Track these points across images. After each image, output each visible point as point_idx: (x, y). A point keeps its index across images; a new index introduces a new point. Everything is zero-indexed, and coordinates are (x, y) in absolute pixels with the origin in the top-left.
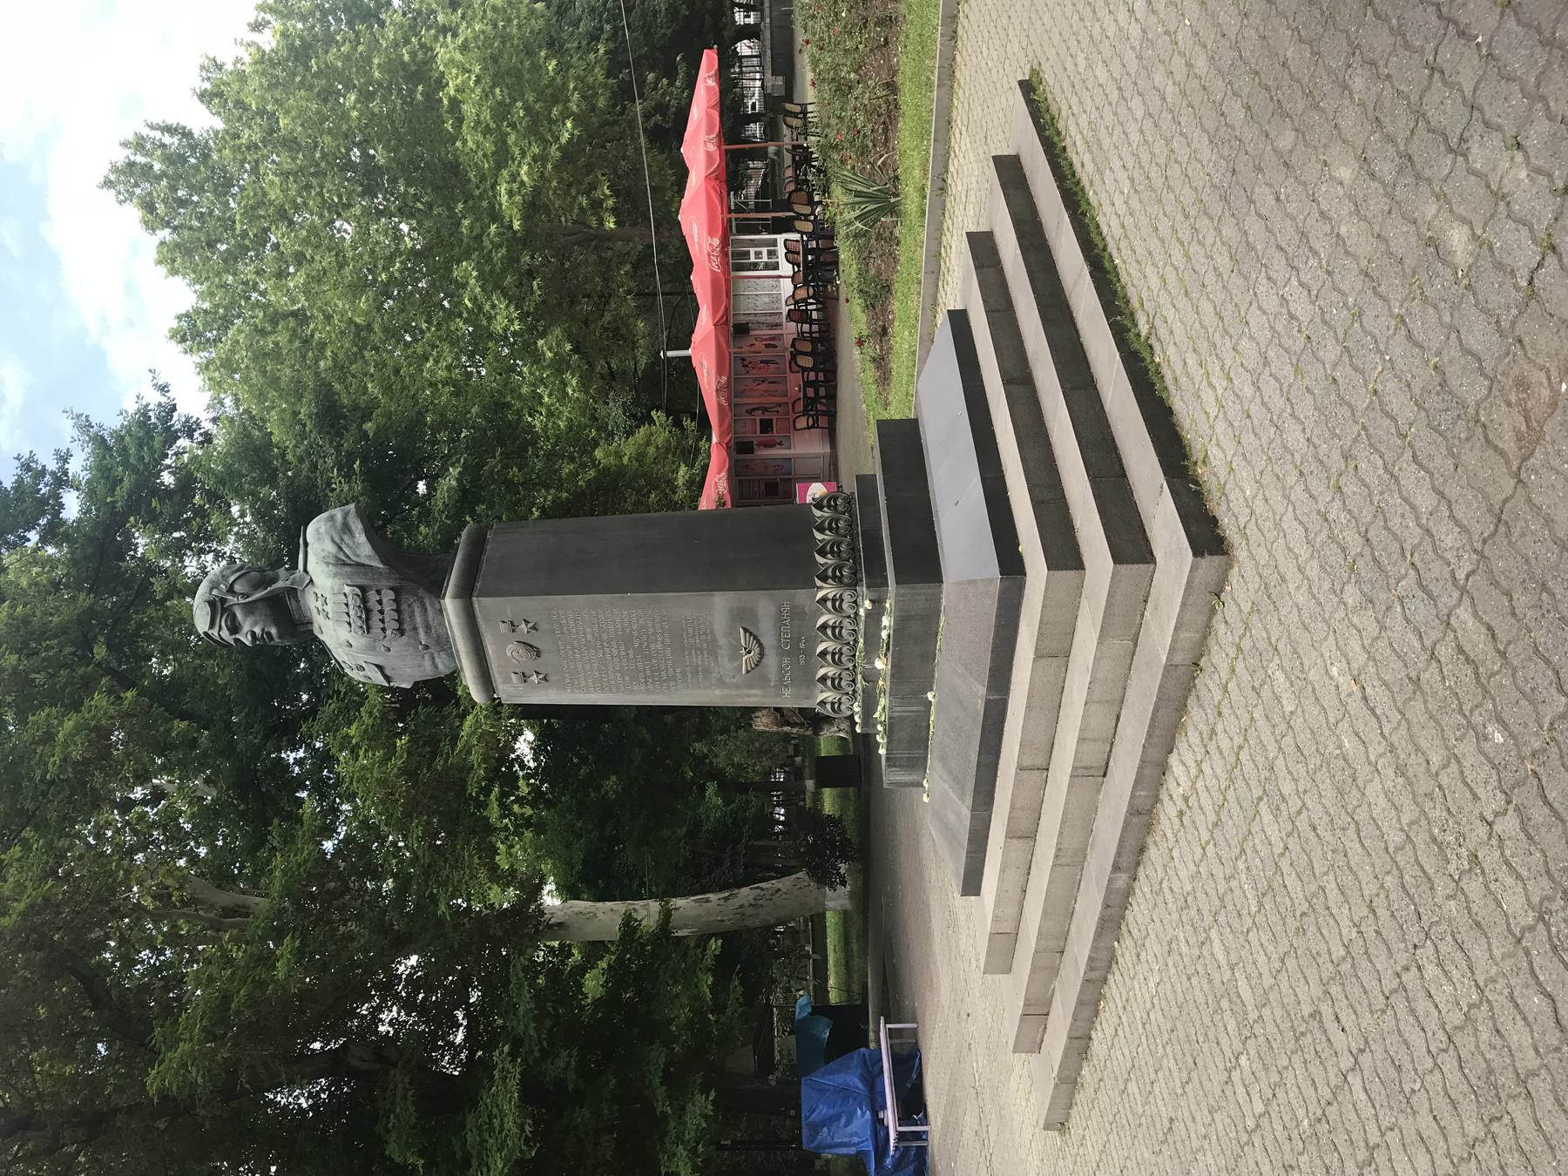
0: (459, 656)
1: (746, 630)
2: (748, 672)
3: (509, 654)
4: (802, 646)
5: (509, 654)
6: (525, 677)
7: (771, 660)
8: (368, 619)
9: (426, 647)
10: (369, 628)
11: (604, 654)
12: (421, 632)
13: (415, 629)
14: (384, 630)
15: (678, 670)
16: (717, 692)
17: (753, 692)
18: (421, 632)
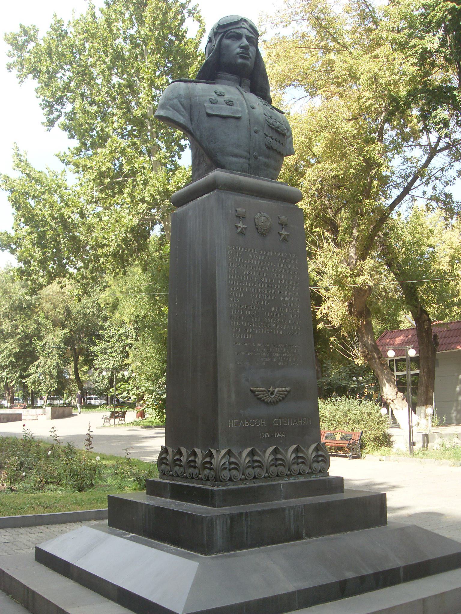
0: (244, 175)
1: (289, 392)
2: (253, 391)
3: (263, 214)
4: (278, 435)
5: (263, 214)
6: (240, 217)
7: (263, 411)
8: (277, 131)
9: (256, 158)
10: (272, 128)
11: (264, 283)
12: (266, 160)
13: (268, 157)
14: (271, 137)
15: (252, 336)
16: (231, 366)
17: (233, 396)
18: (266, 160)
